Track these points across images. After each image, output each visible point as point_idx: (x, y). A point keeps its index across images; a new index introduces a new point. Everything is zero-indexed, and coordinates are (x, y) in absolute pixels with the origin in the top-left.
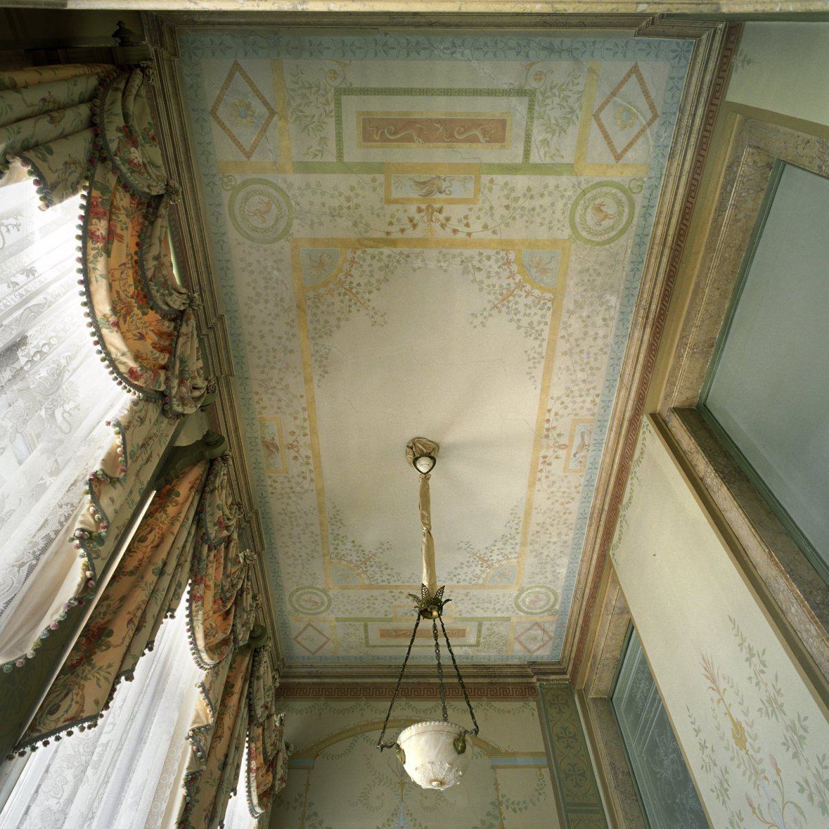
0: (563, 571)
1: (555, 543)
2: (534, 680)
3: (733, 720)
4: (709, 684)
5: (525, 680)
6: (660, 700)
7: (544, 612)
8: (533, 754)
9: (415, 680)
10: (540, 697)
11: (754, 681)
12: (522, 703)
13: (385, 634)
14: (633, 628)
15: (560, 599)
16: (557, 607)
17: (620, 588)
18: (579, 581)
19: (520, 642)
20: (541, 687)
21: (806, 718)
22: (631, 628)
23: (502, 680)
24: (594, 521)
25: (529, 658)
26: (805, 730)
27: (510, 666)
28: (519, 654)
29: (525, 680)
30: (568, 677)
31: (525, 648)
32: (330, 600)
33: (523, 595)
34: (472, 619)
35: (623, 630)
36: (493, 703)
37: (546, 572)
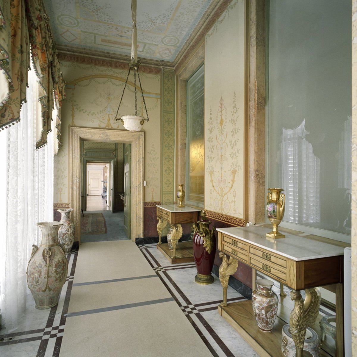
0: (184, 33)
1: (185, 22)
2: (161, 67)
3: (222, 118)
4: (220, 105)
5: (158, 67)
6: (204, 92)
7: (172, 45)
8: (156, 94)
9: (115, 60)
10: (162, 74)
11: (232, 113)
12: (155, 76)
13: (103, 41)
14: (204, 64)
15: (179, 43)
16: (178, 45)
17: (205, 51)
18: (189, 38)
19: (160, 54)
20: (163, 70)
21: (239, 130)
22: (203, 63)
23: (149, 65)
24: (204, 18)
25: (161, 59)
26: (238, 132)
27: (153, 60)
28: (158, 57)
29: (158, 67)
30: (174, 68)
31: (161, 56)
32: (78, 23)
33: (165, 39)
34: (142, 43)
35: (199, 63)
36: (144, 74)
37: (178, 32)
